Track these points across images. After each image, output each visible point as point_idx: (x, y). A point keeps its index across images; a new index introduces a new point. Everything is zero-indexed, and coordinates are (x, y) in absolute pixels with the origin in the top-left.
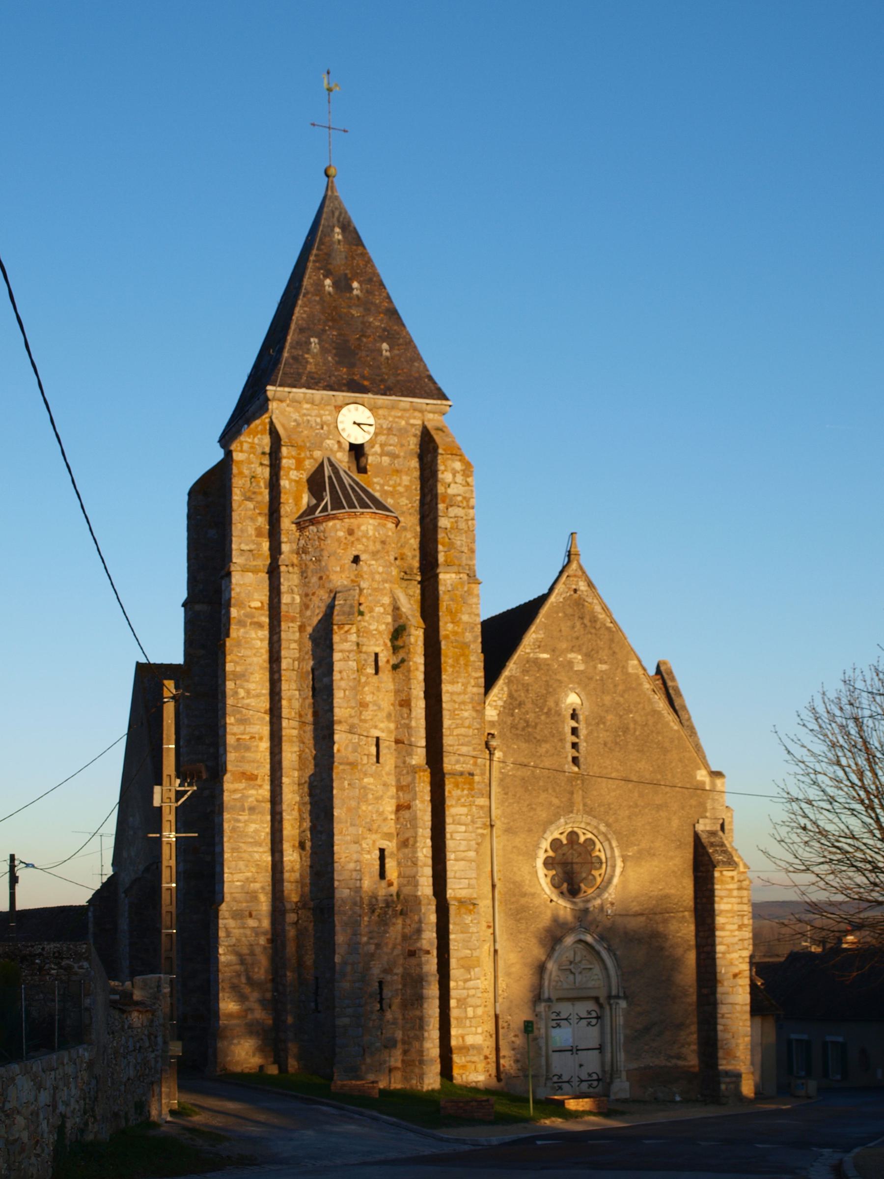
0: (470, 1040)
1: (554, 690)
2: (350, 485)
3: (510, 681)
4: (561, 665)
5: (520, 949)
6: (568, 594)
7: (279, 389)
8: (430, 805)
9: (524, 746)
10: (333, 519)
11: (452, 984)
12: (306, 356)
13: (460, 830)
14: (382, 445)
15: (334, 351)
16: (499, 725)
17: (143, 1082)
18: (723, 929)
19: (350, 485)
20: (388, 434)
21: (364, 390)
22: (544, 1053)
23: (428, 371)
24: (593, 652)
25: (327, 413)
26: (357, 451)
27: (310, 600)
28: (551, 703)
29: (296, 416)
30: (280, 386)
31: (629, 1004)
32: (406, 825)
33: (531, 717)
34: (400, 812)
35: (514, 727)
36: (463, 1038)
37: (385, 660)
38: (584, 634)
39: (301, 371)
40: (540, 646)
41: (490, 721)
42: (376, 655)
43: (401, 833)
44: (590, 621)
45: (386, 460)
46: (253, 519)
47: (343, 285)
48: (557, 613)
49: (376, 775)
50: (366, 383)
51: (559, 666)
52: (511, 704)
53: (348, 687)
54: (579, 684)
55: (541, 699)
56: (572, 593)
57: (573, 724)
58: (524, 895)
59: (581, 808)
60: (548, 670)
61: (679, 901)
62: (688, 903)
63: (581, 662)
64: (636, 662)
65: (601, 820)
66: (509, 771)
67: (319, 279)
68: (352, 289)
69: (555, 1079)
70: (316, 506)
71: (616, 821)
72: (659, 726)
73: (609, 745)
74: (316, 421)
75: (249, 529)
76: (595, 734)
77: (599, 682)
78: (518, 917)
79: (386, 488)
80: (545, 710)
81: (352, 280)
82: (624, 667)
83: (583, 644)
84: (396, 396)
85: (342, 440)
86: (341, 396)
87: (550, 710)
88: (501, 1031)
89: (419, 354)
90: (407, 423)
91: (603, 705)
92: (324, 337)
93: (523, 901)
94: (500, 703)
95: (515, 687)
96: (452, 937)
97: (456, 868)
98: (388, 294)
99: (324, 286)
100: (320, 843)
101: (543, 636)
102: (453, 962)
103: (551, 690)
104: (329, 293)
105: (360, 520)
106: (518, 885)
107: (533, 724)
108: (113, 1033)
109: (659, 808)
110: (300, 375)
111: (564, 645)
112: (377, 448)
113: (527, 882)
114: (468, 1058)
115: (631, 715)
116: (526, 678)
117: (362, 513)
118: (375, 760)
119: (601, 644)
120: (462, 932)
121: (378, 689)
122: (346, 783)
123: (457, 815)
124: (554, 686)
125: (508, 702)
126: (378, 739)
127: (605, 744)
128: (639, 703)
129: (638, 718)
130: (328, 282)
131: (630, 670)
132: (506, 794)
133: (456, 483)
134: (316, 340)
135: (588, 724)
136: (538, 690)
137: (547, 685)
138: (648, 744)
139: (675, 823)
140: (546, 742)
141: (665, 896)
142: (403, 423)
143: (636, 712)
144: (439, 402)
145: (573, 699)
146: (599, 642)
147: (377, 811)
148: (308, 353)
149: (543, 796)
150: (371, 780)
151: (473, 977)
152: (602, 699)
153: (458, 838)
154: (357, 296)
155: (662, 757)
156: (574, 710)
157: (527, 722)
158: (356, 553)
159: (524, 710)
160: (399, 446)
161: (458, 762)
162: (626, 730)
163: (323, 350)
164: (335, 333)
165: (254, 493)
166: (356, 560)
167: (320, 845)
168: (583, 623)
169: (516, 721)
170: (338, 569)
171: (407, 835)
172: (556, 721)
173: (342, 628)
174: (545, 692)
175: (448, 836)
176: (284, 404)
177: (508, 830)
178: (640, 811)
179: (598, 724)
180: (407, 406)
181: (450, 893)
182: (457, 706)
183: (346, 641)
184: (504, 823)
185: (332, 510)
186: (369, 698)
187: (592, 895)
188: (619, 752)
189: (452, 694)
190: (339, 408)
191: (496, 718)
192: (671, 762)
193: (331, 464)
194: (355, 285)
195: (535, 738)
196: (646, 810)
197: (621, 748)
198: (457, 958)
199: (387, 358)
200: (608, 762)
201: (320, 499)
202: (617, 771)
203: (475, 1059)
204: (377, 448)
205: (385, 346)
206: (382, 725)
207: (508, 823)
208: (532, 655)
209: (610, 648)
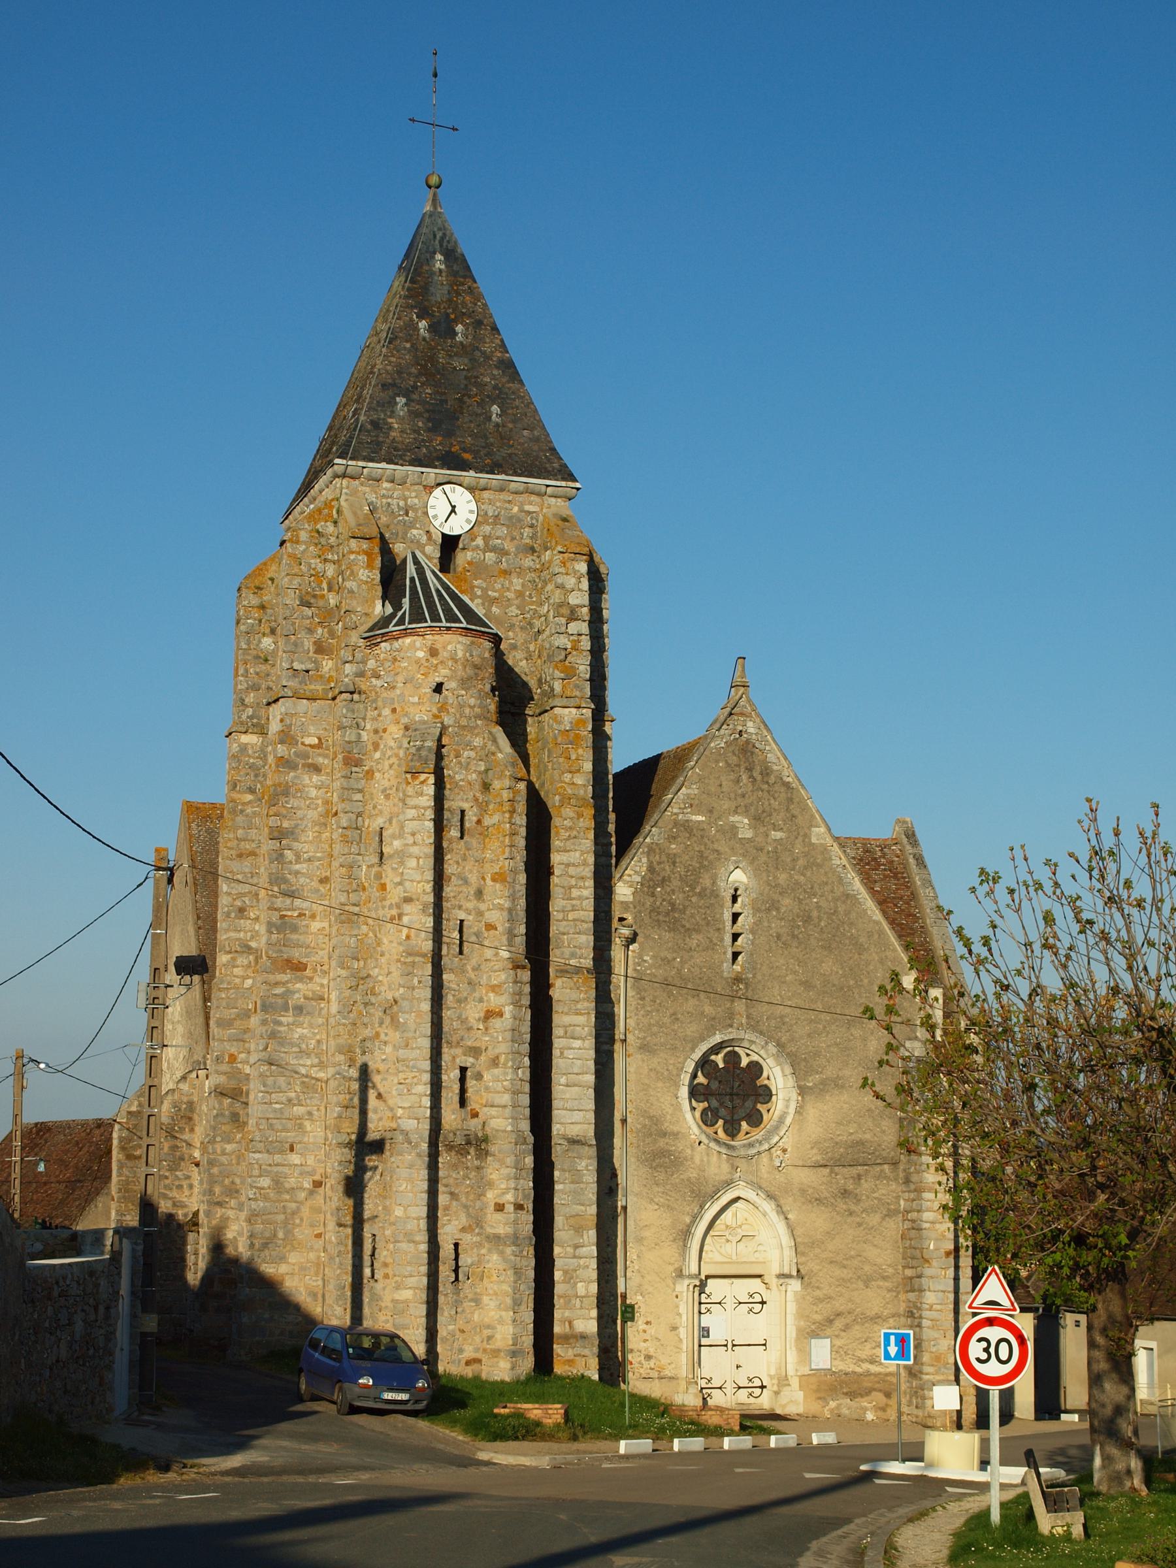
1: (711, 863)
2: (438, 591)
4: (721, 830)
5: (657, 1207)
6: (732, 738)
7: (350, 463)
8: (529, 1011)
9: (667, 936)
10: (411, 634)
11: (557, 1250)
12: (390, 420)
13: (574, 1046)
14: (486, 538)
15: (426, 415)
16: (635, 907)
17: (84, 1365)
19: (438, 591)
20: (495, 524)
21: (463, 466)
23: (551, 442)
24: (765, 814)
25: (413, 494)
26: (450, 544)
27: (381, 738)
28: (706, 881)
29: (372, 498)
30: (352, 459)
31: (805, 1286)
32: (497, 1038)
33: (678, 898)
34: (491, 1020)
35: (654, 910)
36: (570, 1323)
37: (475, 819)
38: (752, 791)
39: (381, 439)
40: (692, 805)
41: (622, 902)
43: (490, 1048)
44: (762, 774)
45: (490, 557)
46: (310, 631)
47: (442, 328)
48: (717, 762)
50: (467, 456)
51: (717, 831)
52: (651, 880)
53: (421, 855)
54: (744, 856)
55: (692, 875)
56: (738, 736)
58: (664, 1134)
59: (744, 1021)
60: (702, 837)
61: (875, 1150)
62: (889, 1153)
63: (746, 827)
64: (823, 830)
65: (770, 1038)
66: (647, 969)
67: (411, 320)
68: (456, 334)
69: (703, 1383)
70: (393, 616)
71: (792, 1040)
72: (853, 915)
73: (784, 939)
74: (398, 505)
75: (306, 643)
76: (766, 924)
77: (771, 855)
78: (654, 1164)
79: (490, 593)
80: (698, 890)
81: (456, 321)
82: (807, 836)
83: (751, 804)
84: (507, 475)
85: (432, 530)
86: (431, 474)
87: (704, 889)
89: (540, 421)
90: (521, 510)
91: (777, 885)
92: (415, 397)
93: (662, 1143)
95: (657, 857)
96: (557, 1187)
97: (568, 1096)
98: (502, 340)
99: (417, 329)
100: (384, 1057)
101: (696, 792)
102: (559, 1221)
103: (706, 863)
104: (424, 339)
105: (447, 637)
106: (656, 1121)
107: (681, 907)
108: (33, 1301)
110: (379, 444)
111: (726, 805)
112: (479, 541)
113: (669, 1117)
114: (578, 1351)
115: (815, 900)
116: (673, 846)
117: (448, 629)
118: (458, 950)
119: (775, 804)
120: (572, 1183)
122: (416, 981)
123: (570, 1025)
124: (711, 857)
125: (647, 877)
126: (462, 921)
127: (779, 937)
128: (827, 883)
129: (823, 904)
130: (423, 324)
131: (814, 840)
132: (643, 999)
133: (579, 590)
134: (404, 400)
136: (689, 863)
137: (701, 855)
138: (837, 939)
140: (698, 931)
141: (857, 1142)
142: (516, 509)
143: (821, 896)
144: (563, 484)
146: (772, 801)
147: (459, 1018)
148: (390, 417)
151: (586, 1242)
152: (775, 877)
153: (571, 1057)
154: (461, 343)
155: (856, 956)
157: (673, 905)
158: (438, 680)
159: (668, 889)
160: (509, 539)
161: (573, 955)
162: (807, 919)
163: (413, 414)
164: (428, 391)
165: (315, 596)
166: (438, 688)
167: (384, 1060)
168: (751, 776)
169: (658, 903)
170: (416, 699)
171: (497, 1051)
172: (712, 905)
173: (417, 778)
174: (698, 865)
175: (556, 1052)
176: (357, 482)
177: (644, 1048)
178: (825, 1027)
179: (769, 910)
180: (521, 487)
181: (556, 1129)
182: (573, 882)
183: (422, 794)
184: (638, 1038)
185: (409, 623)
187: (757, 1137)
188: (797, 948)
189: (568, 865)
190: (430, 489)
191: (631, 898)
192: (868, 964)
193: (416, 562)
194: (459, 328)
195: (684, 926)
196: (833, 1027)
197: (800, 943)
198: (565, 1216)
199: (497, 425)
200: (782, 961)
201: (397, 606)
202: (795, 972)
203: (586, 1352)
204: (479, 541)
205: (495, 408)
206: (470, 905)
207: (645, 1038)
208: (680, 817)
209: (788, 810)
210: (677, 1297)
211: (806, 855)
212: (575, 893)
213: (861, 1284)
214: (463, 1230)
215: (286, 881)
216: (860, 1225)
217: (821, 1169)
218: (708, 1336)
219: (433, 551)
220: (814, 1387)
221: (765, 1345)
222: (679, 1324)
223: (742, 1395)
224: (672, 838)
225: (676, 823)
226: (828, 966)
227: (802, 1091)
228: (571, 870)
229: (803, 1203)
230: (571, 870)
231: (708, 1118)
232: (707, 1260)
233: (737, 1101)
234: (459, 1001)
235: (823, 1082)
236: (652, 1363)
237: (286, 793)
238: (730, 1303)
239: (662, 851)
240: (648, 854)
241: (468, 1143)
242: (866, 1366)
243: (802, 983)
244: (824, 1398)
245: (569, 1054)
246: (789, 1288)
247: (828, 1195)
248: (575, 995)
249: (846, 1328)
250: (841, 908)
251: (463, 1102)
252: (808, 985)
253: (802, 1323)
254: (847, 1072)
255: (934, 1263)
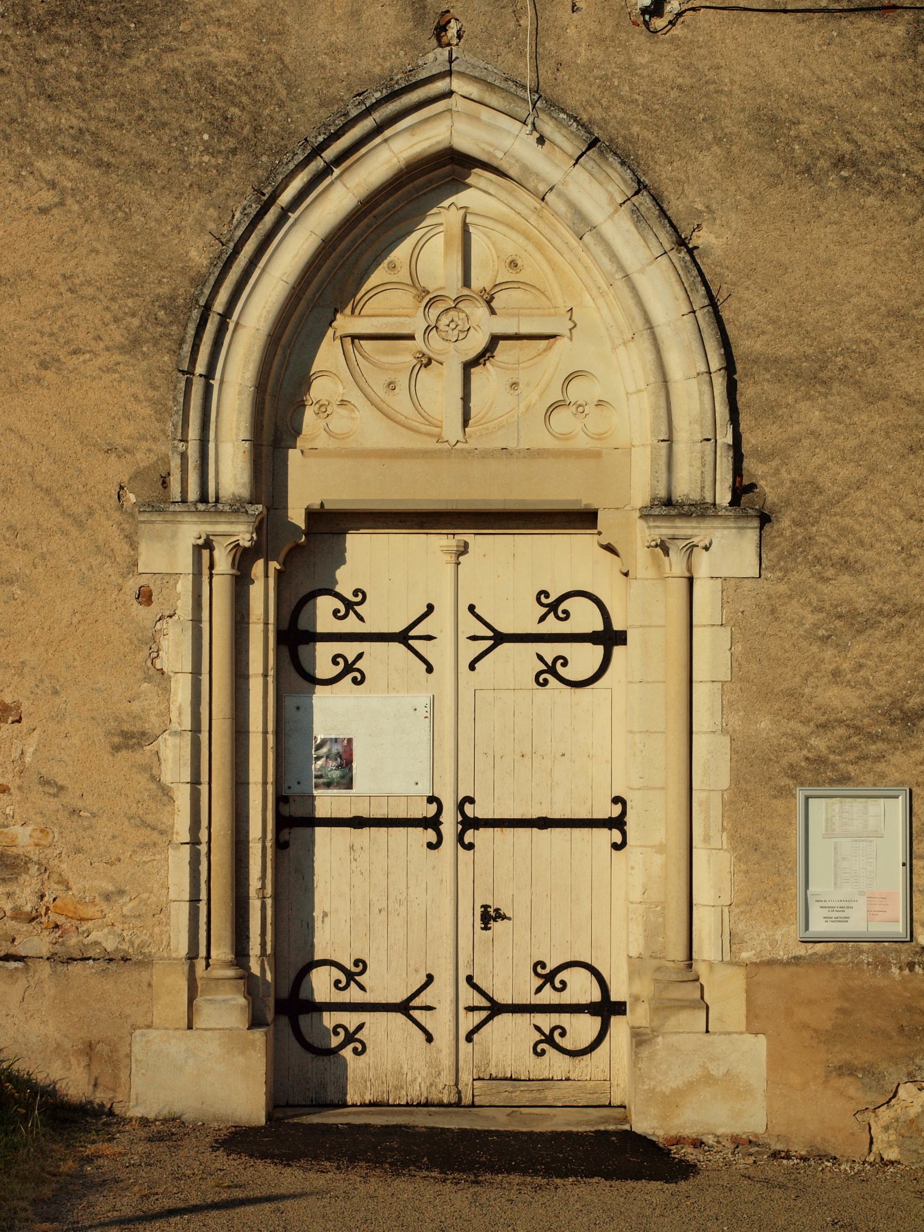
5: (47, 197)
210: (145, 596)
217: (866, 22)
218: (347, 782)
220: (823, 1018)
221: (618, 823)
222: (152, 723)
229: (775, 180)
232: (322, 442)
244: (869, 1070)
246: (704, 565)
247: (898, 142)
253: (764, 724)
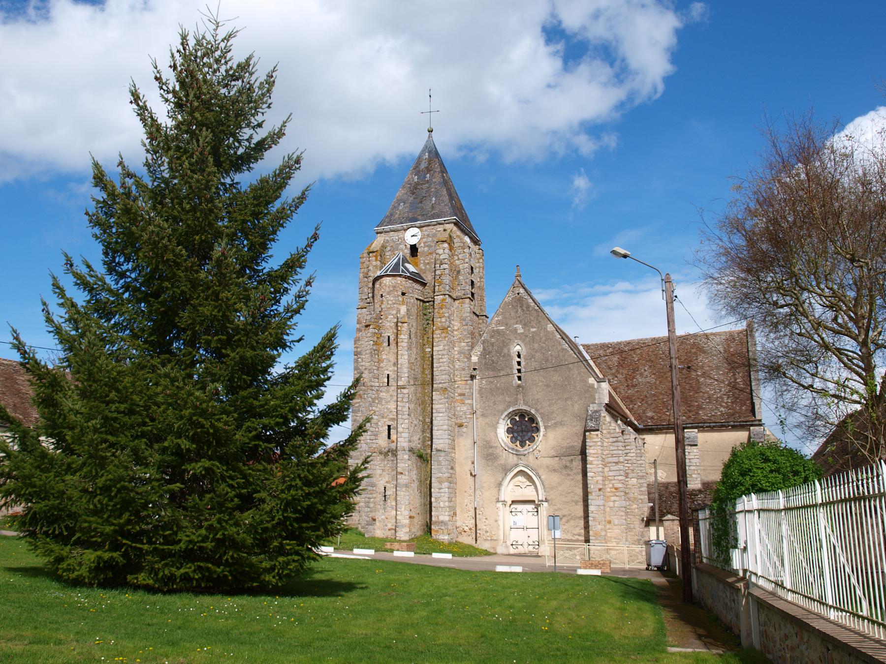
0: (441, 518)
3: (484, 342)
18: (591, 464)
21: (416, 220)
22: (501, 527)
28: (505, 351)
31: (549, 505)
35: (486, 364)
42: (389, 337)
45: (426, 249)
49: (388, 391)
57: (518, 360)
58: (491, 447)
71: (542, 407)
72: (566, 357)
88: (478, 516)
93: (490, 451)
94: (479, 353)
109: (566, 399)
110: (390, 220)
111: (513, 321)
112: (422, 245)
119: (532, 318)
121: (389, 353)
135: (526, 359)
139: (577, 407)
145: (518, 348)
149: (501, 397)
150: (384, 394)
156: (518, 353)
157: (493, 361)
177: (483, 415)
186: (384, 357)
190: (405, 230)
192: (573, 375)
202: (542, 382)
203: (443, 528)
204: (422, 245)
205: (434, 199)
209: (537, 319)
211: (545, 336)
212: (441, 360)
213: (574, 504)
214: (387, 482)
215: (359, 369)
216: (572, 479)
219: (408, 252)
223: (531, 548)
224: (492, 337)
225: (493, 331)
226: (556, 378)
227: (546, 428)
228: (440, 353)
230: (440, 353)
231: (513, 440)
233: (525, 433)
234: (387, 402)
235: (555, 423)
236: (488, 534)
237: (359, 340)
238: (525, 512)
239: (488, 342)
240: (483, 344)
241: (389, 451)
242: (577, 537)
243: (545, 385)
245: (438, 419)
248: (440, 397)
249: (568, 521)
250: (561, 354)
251: (389, 437)
252: (548, 386)
254: (565, 419)
255: (593, 494)
